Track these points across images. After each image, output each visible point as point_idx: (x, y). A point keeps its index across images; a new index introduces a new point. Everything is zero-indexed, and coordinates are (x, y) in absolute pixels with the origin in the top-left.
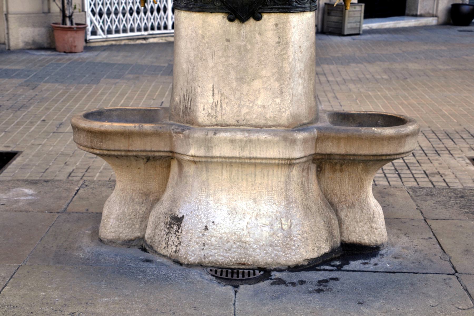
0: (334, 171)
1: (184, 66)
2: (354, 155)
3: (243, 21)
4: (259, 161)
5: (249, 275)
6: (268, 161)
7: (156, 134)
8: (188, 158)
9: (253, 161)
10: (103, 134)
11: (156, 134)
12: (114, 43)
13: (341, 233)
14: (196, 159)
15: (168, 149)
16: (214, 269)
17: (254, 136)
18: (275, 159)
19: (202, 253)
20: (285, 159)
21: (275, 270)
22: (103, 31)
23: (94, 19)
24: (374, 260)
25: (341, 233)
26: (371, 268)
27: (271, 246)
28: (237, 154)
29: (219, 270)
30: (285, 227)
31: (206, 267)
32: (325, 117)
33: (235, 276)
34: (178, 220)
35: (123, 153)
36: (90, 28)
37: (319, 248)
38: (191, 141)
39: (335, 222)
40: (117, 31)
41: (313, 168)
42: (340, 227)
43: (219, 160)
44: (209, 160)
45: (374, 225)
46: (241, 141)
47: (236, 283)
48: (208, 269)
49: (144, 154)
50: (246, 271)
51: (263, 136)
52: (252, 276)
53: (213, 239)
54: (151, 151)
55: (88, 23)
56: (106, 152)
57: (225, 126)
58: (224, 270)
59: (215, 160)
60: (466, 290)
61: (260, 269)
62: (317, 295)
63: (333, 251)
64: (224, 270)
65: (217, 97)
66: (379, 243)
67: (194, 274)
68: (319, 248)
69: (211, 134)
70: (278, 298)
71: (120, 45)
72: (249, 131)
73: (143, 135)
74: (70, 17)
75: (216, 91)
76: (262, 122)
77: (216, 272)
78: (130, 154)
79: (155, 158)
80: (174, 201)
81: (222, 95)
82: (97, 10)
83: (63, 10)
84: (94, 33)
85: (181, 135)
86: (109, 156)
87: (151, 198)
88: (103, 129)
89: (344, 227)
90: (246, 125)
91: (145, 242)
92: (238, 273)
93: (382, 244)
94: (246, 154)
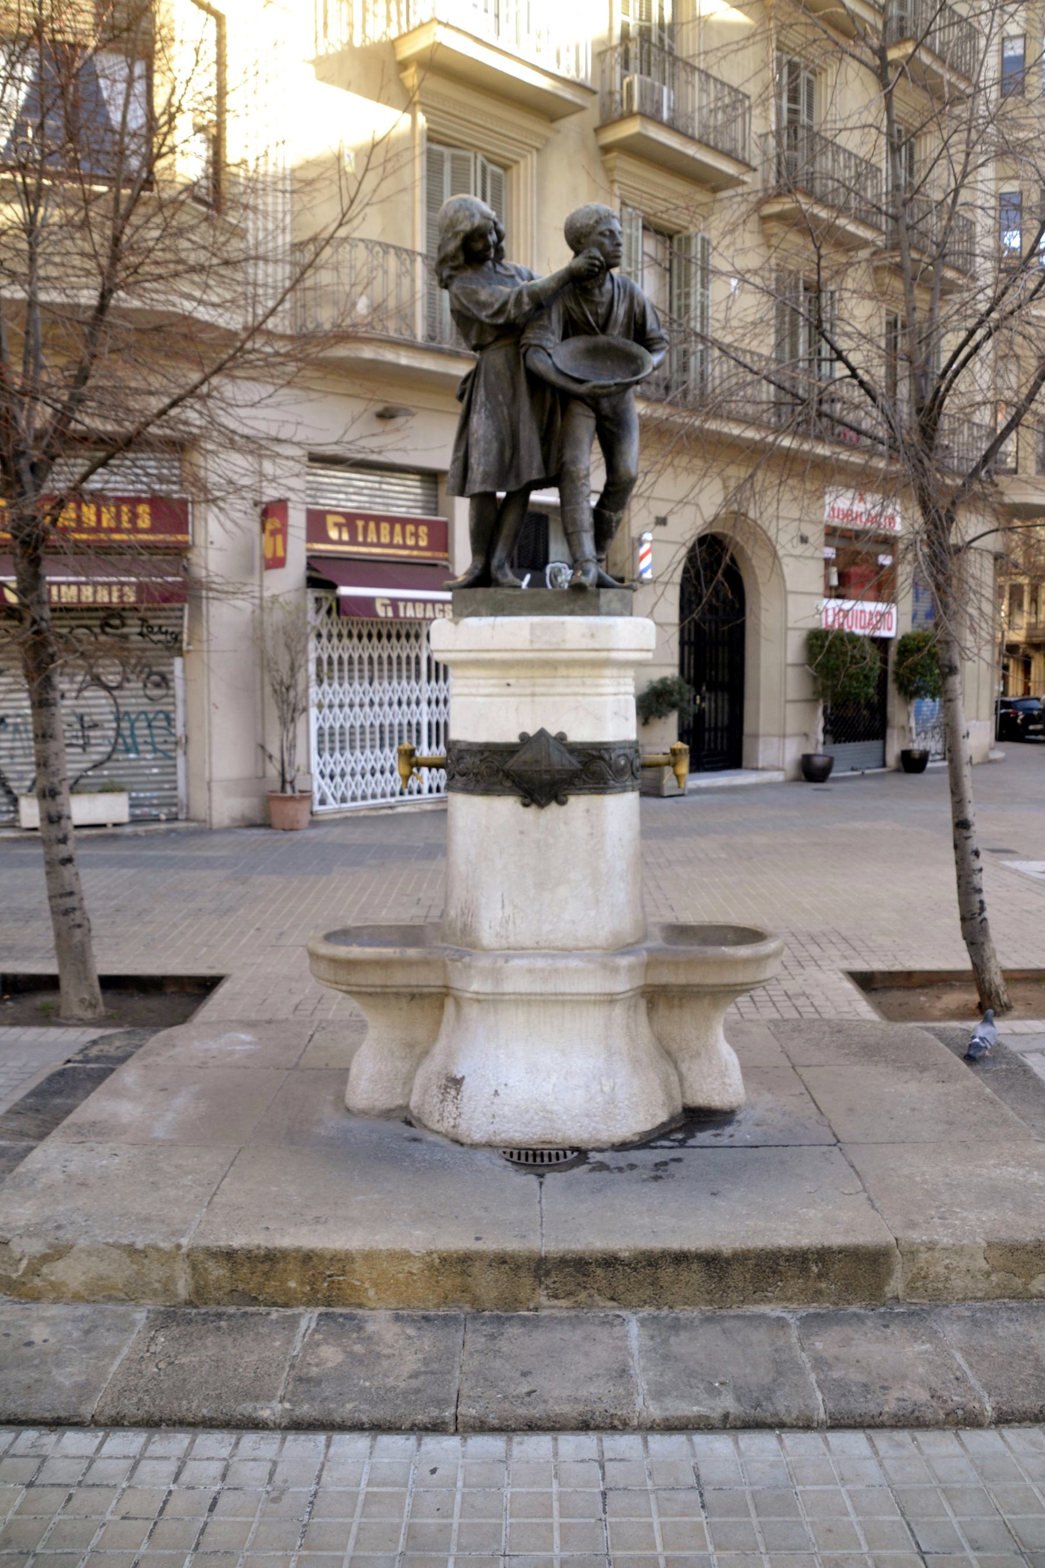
0: (671, 1007)
1: (463, 868)
2: (698, 986)
3: (541, 806)
4: (569, 998)
5: (558, 1158)
6: (580, 998)
7: (426, 963)
8: (468, 995)
9: (560, 998)
10: (351, 964)
11: (426, 963)
12: (349, 814)
13: (683, 1093)
14: (481, 997)
15: (440, 983)
16: (508, 1151)
17: (561, 964)
18: (590, 994)
19: (491, 1128)
20: (595, 994)
21: (594, 1149)
22: (335, 798)
23: (322, 783)
24: (728, 1130)
25: (683, 1093)
26: (725, 1141)
27: (587, 1115)
28: (537, 987)
29: (515, 1152)
30: (606, 1089)
31: (497, 1147)
32: (656, 932)
33: (538, 1159)
34: (457, 1083)
35: (379, 990)
36: (317, 796)
37: (654, 1116)
38: (473, 972)
39: (674, 1079)
40: (354, 799)
41: (643, 1004)
42: (681, 1085)
43: (513, 997)
44: (499, 997)
45: (727, 1080)
46: (543, 970)
47: (540, 1171)
48: (501, 1151)
49: (408, 990)
50: (553, 1153)
51: (573, 963)
52: (562, 1160)
53: (506, 1108)
54: (417, 986)
55: (315, 789)
56: (355, 989)
57: (519, 950)
58: (523, 1152)
59: (507, 997)
60: (853, 1167)
61: (573, 1149)
62: (654, 1185)
63: (672, 1119)
64: (523, 1152)
65: (509, 910)
66: (735, 1105)
67: (481, 1158)
68: (654, 1116)
69: (500, 962)
70: (600, 1191)
71: (358, 818)
72: (553, 956)
73: (409, 964)
74: (292, 782)
75: (506, 902)
76: (570, 943)
77: (511, 1154)
78: (388, 990)
79: (422, 996)
80: (450, 1055)
81: (515, 907)
82: (327, 772)
83: (283, 774)
84: (323, 802)
85: (459, 964)
86: (359, 993)
87: (418, 1050)
88: (351, 956)
89: (687, 1085)
90: (549, 948)
91: (411, 1112)
92: (542, 1155)
93: (739, 1107)
94: (550, 988)
